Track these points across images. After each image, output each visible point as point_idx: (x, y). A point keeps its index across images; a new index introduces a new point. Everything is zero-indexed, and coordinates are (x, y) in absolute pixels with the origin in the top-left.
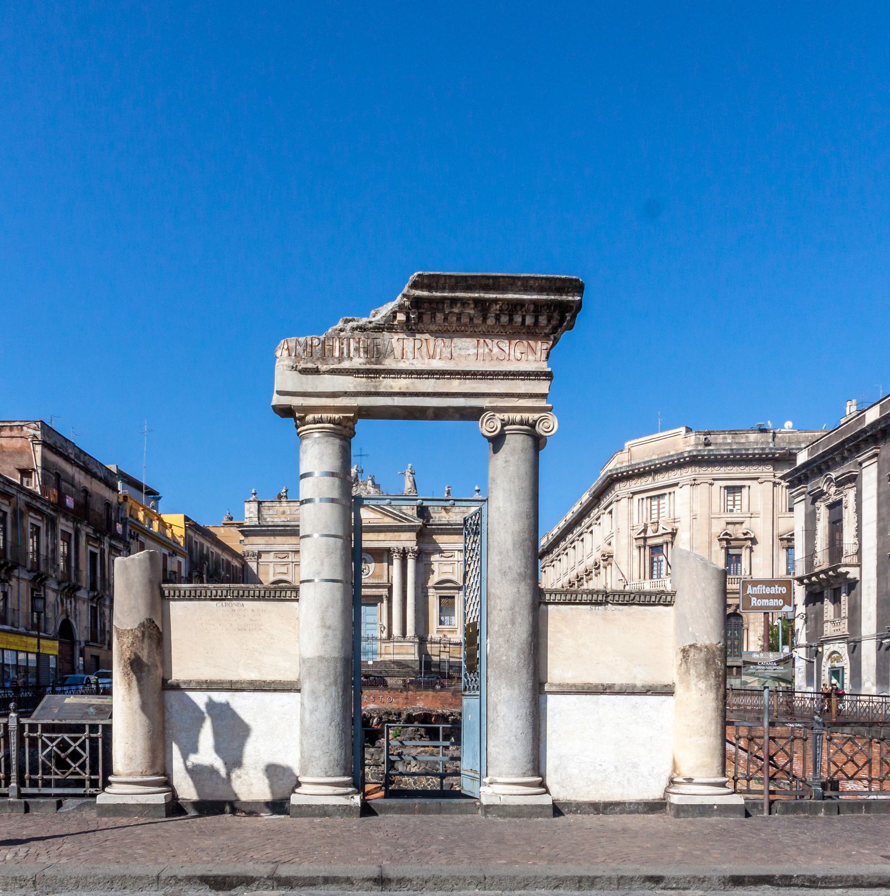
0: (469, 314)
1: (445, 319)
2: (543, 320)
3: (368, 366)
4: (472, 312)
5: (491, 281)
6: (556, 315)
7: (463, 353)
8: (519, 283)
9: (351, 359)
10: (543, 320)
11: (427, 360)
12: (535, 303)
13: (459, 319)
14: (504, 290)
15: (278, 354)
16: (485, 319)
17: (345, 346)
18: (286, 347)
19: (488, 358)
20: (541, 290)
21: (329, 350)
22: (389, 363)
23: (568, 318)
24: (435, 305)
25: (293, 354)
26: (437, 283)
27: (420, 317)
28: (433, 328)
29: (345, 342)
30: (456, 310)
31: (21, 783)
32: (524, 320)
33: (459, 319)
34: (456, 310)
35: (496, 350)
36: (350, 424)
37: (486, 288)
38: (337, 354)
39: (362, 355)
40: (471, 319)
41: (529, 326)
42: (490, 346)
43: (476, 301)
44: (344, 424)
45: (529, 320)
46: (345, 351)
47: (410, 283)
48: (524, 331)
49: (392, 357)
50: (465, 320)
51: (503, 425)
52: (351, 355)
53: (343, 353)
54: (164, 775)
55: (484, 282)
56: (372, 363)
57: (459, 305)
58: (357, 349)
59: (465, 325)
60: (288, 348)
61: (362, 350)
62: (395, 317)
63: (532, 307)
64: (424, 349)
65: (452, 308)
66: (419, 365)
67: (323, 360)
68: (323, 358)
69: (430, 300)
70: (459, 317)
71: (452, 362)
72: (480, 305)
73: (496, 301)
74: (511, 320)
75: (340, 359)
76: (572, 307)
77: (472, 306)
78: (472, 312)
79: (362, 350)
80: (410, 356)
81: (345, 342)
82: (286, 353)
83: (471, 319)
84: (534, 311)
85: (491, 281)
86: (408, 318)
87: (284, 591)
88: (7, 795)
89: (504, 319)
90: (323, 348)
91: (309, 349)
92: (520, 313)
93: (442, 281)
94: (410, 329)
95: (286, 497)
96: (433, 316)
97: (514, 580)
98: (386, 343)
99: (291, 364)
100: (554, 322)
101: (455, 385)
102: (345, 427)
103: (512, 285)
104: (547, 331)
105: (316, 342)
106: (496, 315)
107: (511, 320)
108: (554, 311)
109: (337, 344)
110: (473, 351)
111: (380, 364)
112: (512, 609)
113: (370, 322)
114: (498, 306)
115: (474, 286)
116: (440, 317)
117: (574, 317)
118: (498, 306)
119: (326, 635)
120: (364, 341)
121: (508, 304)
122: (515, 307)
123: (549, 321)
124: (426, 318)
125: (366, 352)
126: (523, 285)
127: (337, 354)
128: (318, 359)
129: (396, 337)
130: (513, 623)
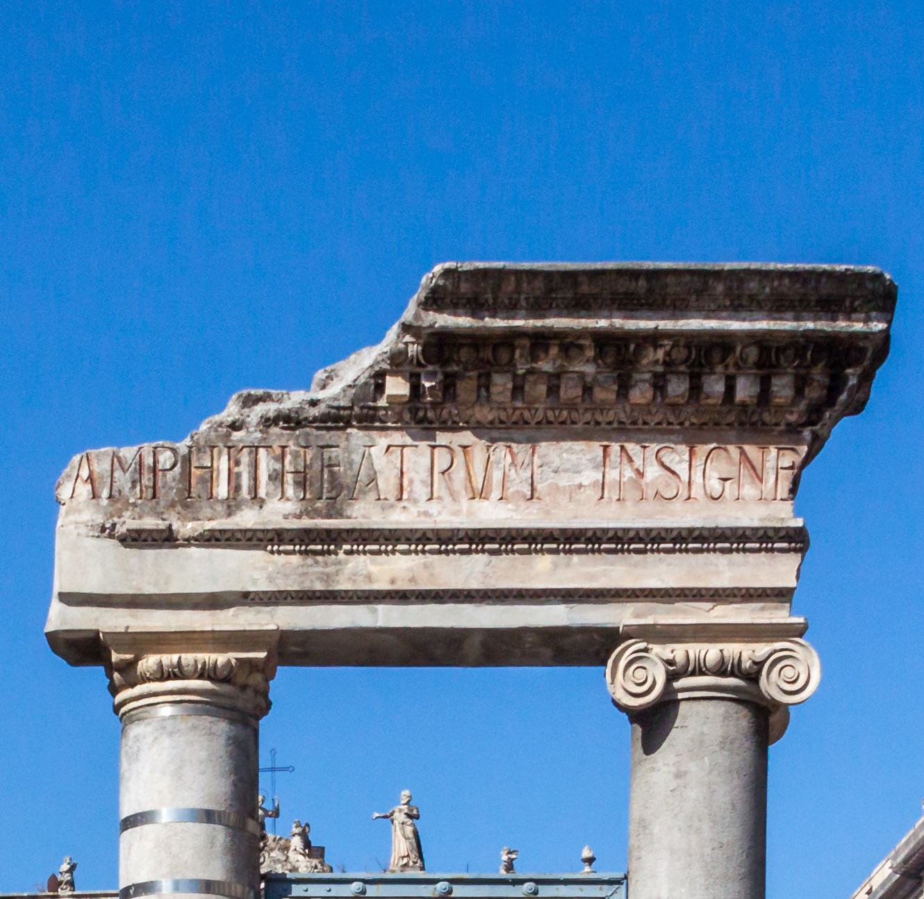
0: (582, 375)
1: (518, 390)
2: (782, 388)
3: (306, 523)
4: (589, 369)
5: (642, 283)
6: (818, 374)
7: (564, 481)
8: (720, 288)
9: (262, 503)
10: (782, 388)
11: (465, 503)
12: (760, 340)
13: (553, 390)
14: (679, 308)
15: (64, 493)
16: (624, 388)
17: (244, 470)
18: (85, 473)
19: (631, 495)
20: (778, 306)
21: (202, 480)
22: (363, 514)
23: (853, 381)
24: (489, 352)
25: (105, 493)
26: (496, 290)
27: (448, 386)
28: (484, 414)
29: (245, 458)
30: (546, 366)
33: (553, 390)
34: (546, 366)
36: (257, 678)
37: (630, 304)
39: (290, 491)
40: (587, 390)
41: (744, 405)
42: (638, 462)
43: (603, 340)
44: (241, 679)
45: (745, 390)
46: (245, 482)
47: (421, 294)
48: (731, 418)
49: (372, 496)
50: (570, 391)
52: (262, 493)
53: (238, 488)
55: (623, 285)
56: (316, 513)
57: (554, 351)
58: (277, 477)
59: (571, 406)
60: (91, 479)
61: (289, 478)
62: (380, 388)
63: (753, 353)
64: (459, 473)
65: (535, 359)
66: (444, 517)
67: (186, 506)
68: (186, 501)
69: (475, 340)
70: (554, 382)
71: (535, 506)
72: (611, 351)
73: (654, 338)
74: (696, 390)
75: (232, 505)
76: (863, 351)
77: (590, 353)
78: (589, 369)
79: (289, 478)
80: (421, 492)
81: (245, 458)
82: (84, 490)
83: (587, 390)
84: (759, 365)
85: (642, 283)
86: (416, 389)
89: (678, 388)
90: (186, 475)
91: (147, 479)
92: (719, 369)
93: (510, 286)
94: (421, 418)
95: (71, 884)
96: (485, 383)
98: (356, 458)
99: (100, 519)
100: (814, 393)
101: (543, 570)
102: (244, 687)
103: (699, 293)
104: (792, 418)
105: (165, 459)
106: (656, 375)
107: (696, 390)
108: (814, 363)
109: (223, 464)
111: (340, 515)
113: (314, 403)
114: (660, 354)
115: (595, 297)
116: (501, 384)
117: (867, 378)
118: (660, 354)
120: (296, 455)
121: (688, 347)
125: (302, 484)
126: (728, 293)
128: (172, 505)
129: (382, 440)
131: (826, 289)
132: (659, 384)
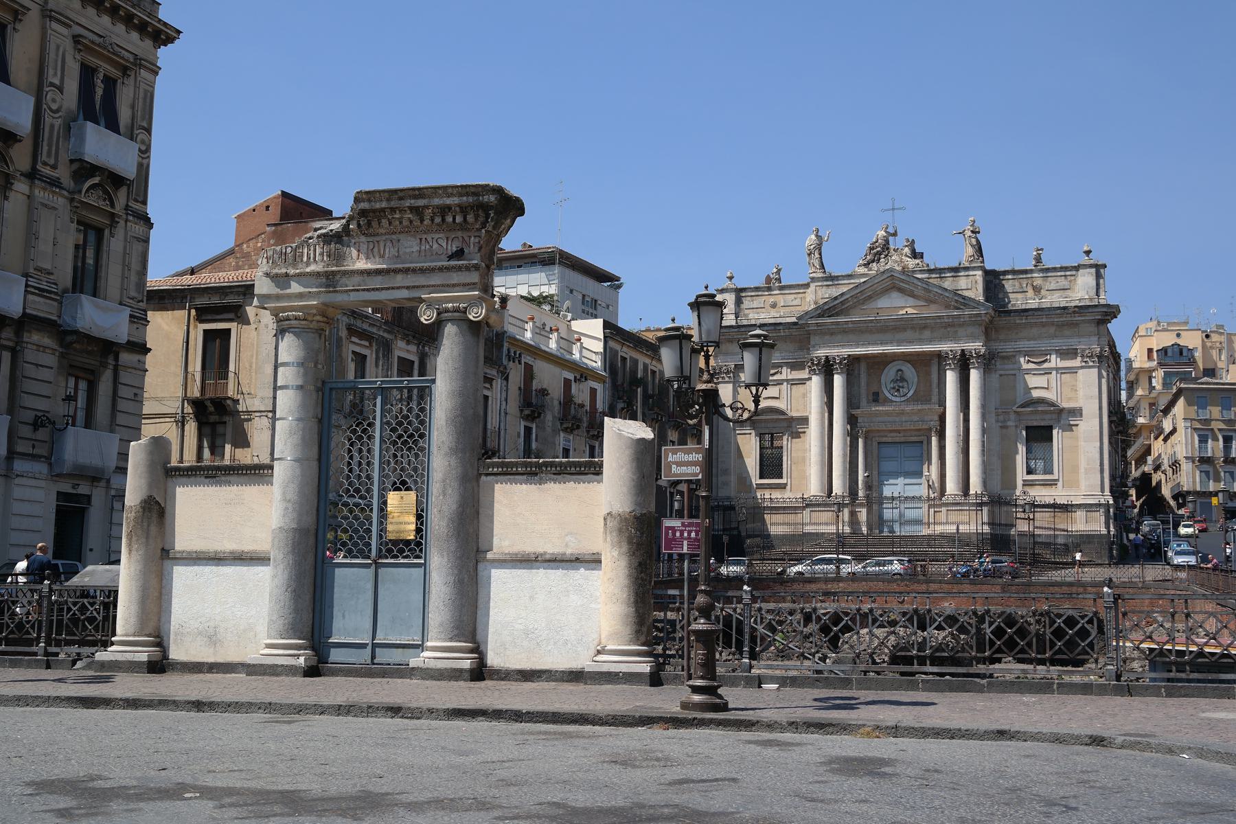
1: (390, 223)
2: (470, 218)
10: (470, 218)
12: (459, 206)
16: (422, 221)
17: (312, 252)
20: (461, 195)
31: (48, 643)
32: (454, 219)
35: (435, 246)
37: (415, 197)
38: (305, 259)
40: (411, 222)
41: (460, 224)
45: (459, 219)
50: (405, 223)
51: (438, 314)
54: (158, 637)
58: (322, 254)
64: (376, 250)
68: (294, 263)
73: (427, 207)
74: (443, 220)
75: (308, 264)
82: (265, 261)
87: (258, 472)
88: (35, 654)
89: (438, 220)
97: (446, 454)
100: (481, 219)
105: (289, 250)
107: (443, 220)
110: (416, 248)
112: (444, 481)
116: (384, 222)
119: (286, 508)
122: (444, 210)
123: (476, 220)
124: (375, 224)
125: (329, 256)
127: (305, 259)
130: (444, 495)
131: (473, 190)
132: (432, 220)
